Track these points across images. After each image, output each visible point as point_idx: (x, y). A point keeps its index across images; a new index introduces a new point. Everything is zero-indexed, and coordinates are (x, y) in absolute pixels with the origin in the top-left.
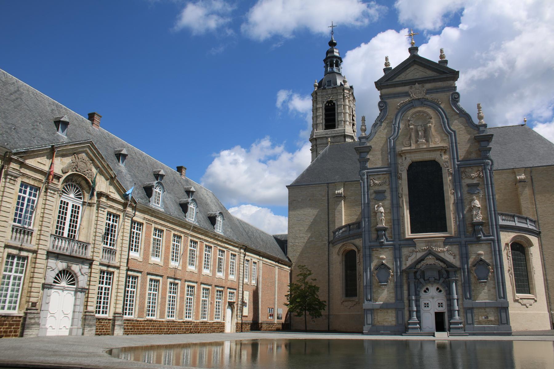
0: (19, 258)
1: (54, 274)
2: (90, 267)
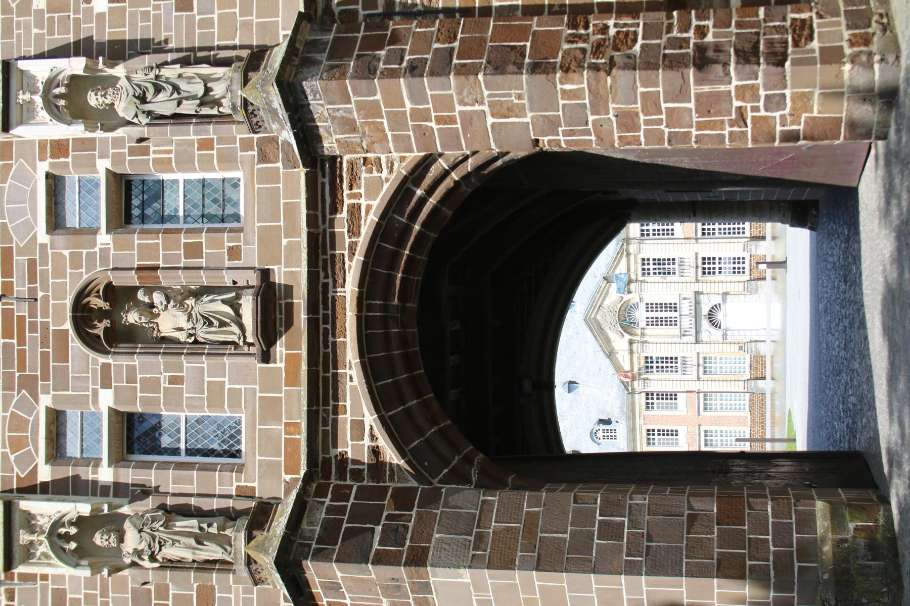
0: (705, 363)
1: (712, 330)
2: (702, 293)
